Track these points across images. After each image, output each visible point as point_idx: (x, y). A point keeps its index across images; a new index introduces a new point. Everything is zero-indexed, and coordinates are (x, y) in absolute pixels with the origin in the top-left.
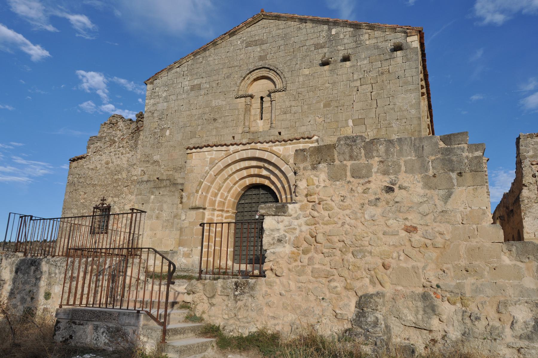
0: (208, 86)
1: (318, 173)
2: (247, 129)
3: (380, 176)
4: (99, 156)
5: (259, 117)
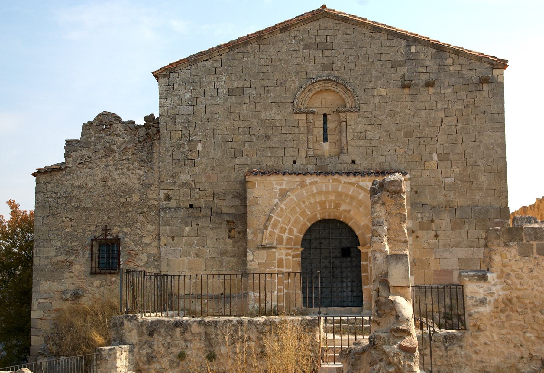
0: (254, 92)
1: (510, 249)
2: (311, 153)
4: (87, 170)
5: (322, 138)
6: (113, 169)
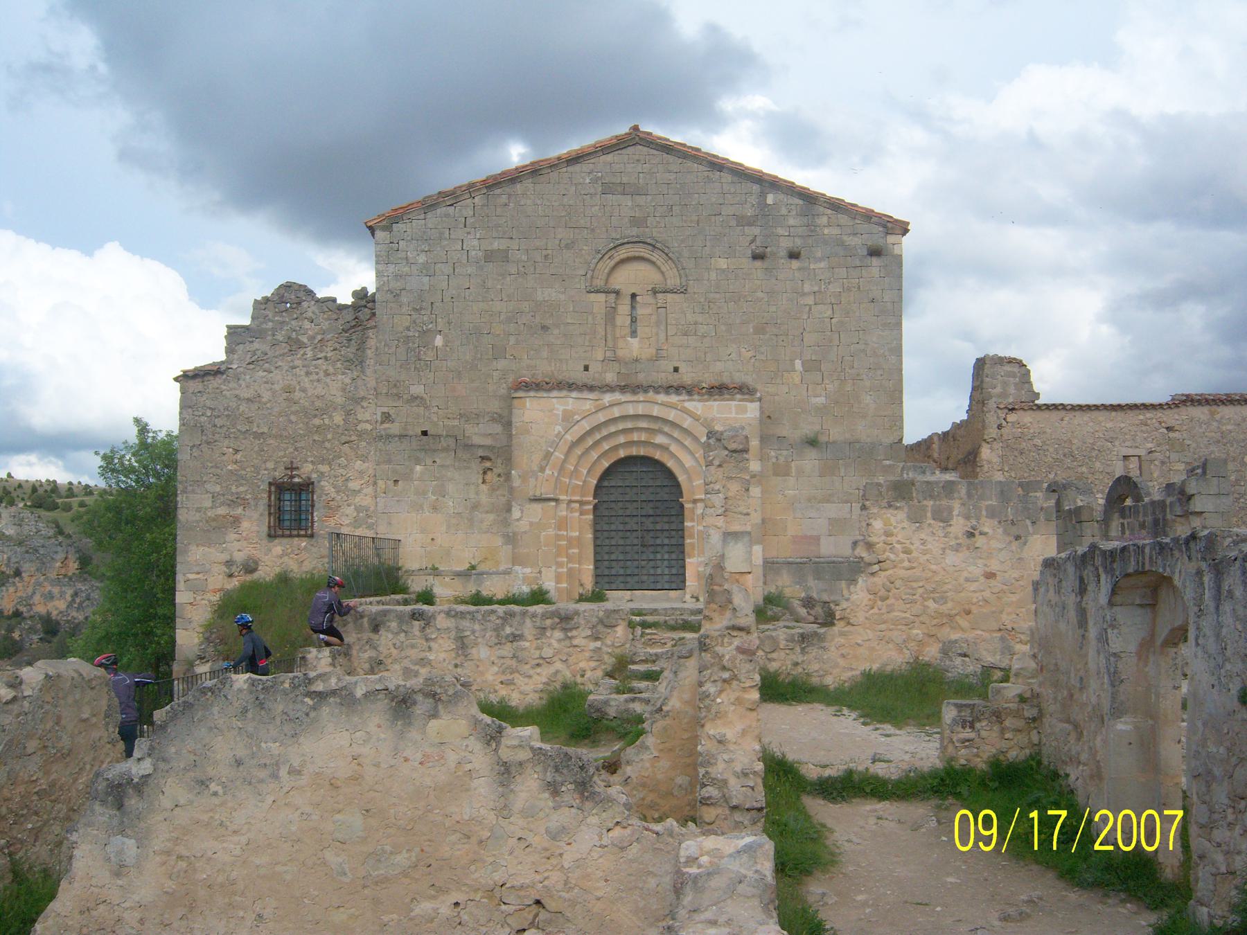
0: (524, 258)
3: (961, 521)
4: (261, 373)
5: (628, 330)
6: (303, 373)
